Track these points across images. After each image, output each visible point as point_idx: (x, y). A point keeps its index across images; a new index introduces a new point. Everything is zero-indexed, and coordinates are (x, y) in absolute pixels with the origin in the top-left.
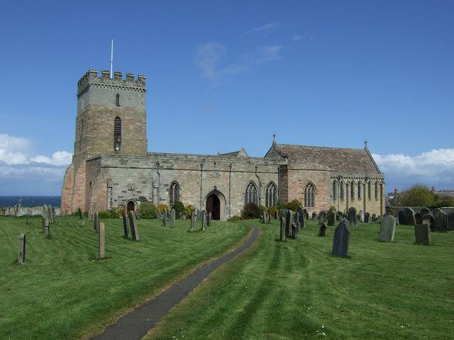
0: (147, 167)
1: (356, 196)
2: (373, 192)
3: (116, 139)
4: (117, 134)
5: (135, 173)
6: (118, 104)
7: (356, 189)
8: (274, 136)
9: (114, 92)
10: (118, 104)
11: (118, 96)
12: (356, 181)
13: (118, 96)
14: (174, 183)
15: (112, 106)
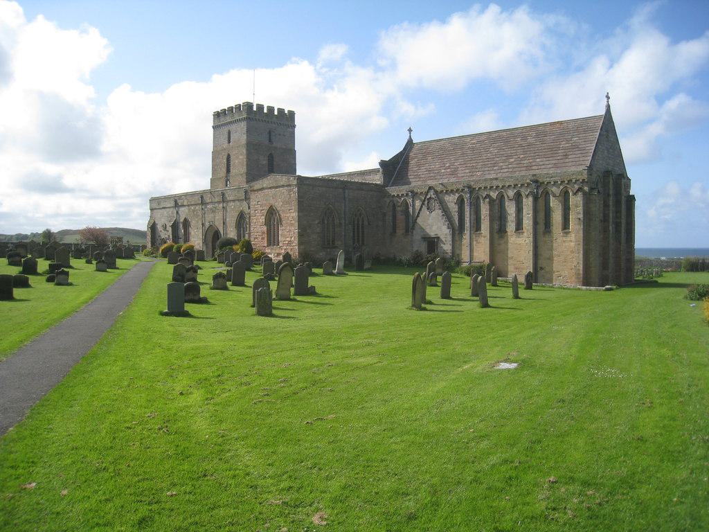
0: (169, 205)
1: (511, 227)
2: (557, 217)
3: (226, 177)
4: (228, 171)
5: (165, 212)
6: (229, 142)
7: (511, 209)
8: (410, 130)
9: (225, 130)
10: (229, 142)
11: (229, 133)
12: (511, 193)
13: (229, 133)
14: (185, 219)
15: (226, 145)
